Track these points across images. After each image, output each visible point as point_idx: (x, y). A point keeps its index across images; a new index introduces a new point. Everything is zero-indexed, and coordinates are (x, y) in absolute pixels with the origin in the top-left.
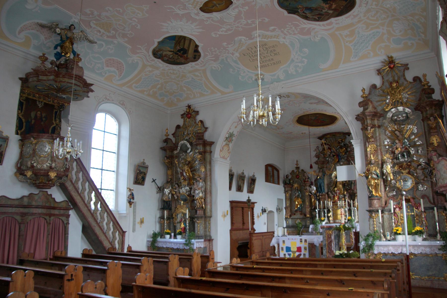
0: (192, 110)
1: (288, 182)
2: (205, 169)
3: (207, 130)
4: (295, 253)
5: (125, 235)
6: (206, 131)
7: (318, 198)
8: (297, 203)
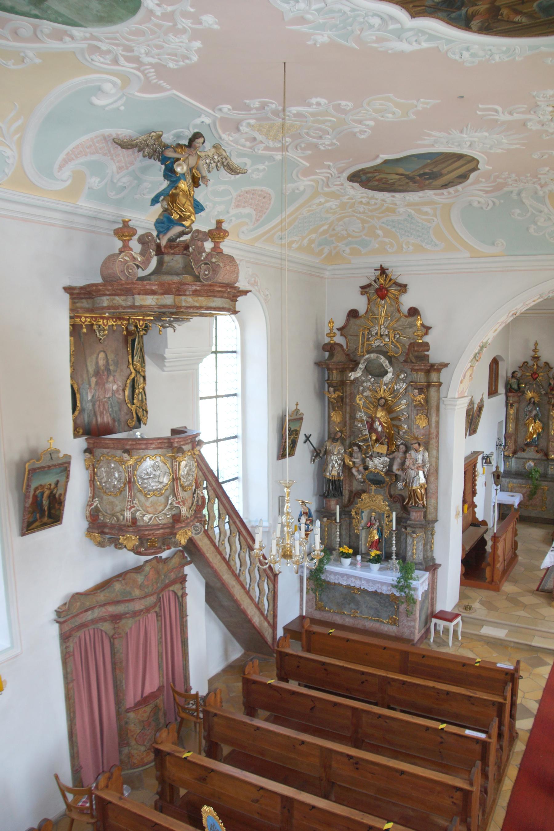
0: (390, 280)
1: (515, 386)
2: (428, 422)
3: (430, 331)
6: (426, 334)
8: (531, 429)
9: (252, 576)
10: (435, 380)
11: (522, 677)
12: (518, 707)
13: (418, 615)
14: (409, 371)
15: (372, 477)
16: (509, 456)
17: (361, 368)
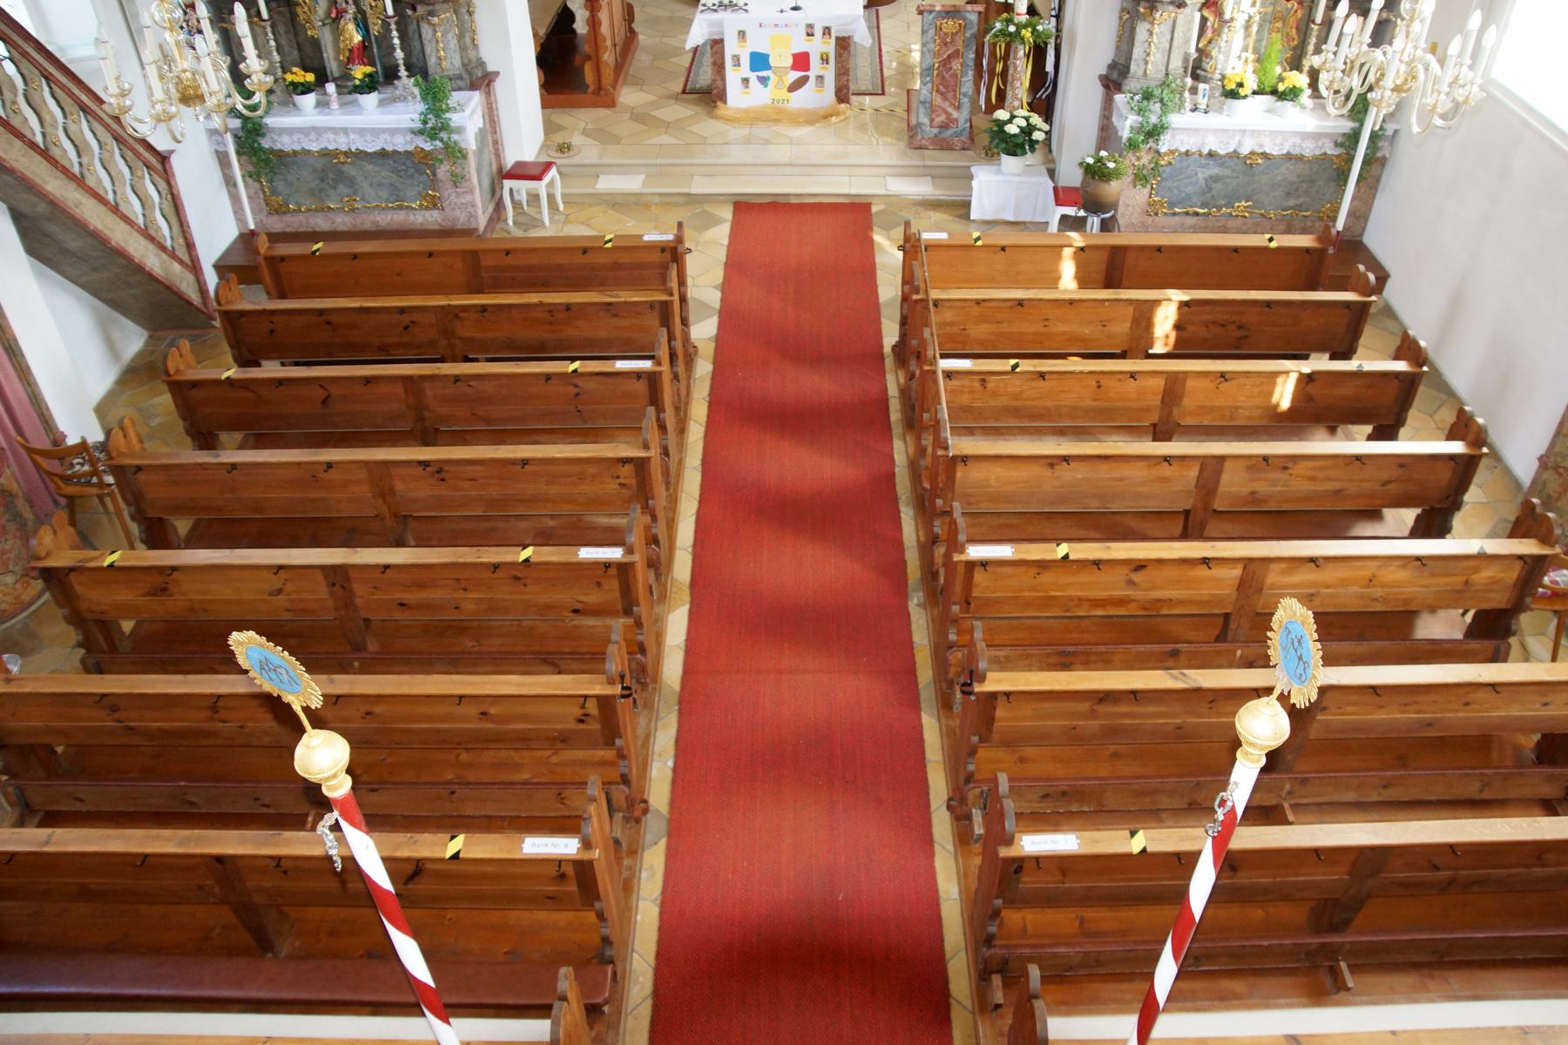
4: (787, 73)
5: (171, 167)
9: (113, 174)
12: (691, 303)
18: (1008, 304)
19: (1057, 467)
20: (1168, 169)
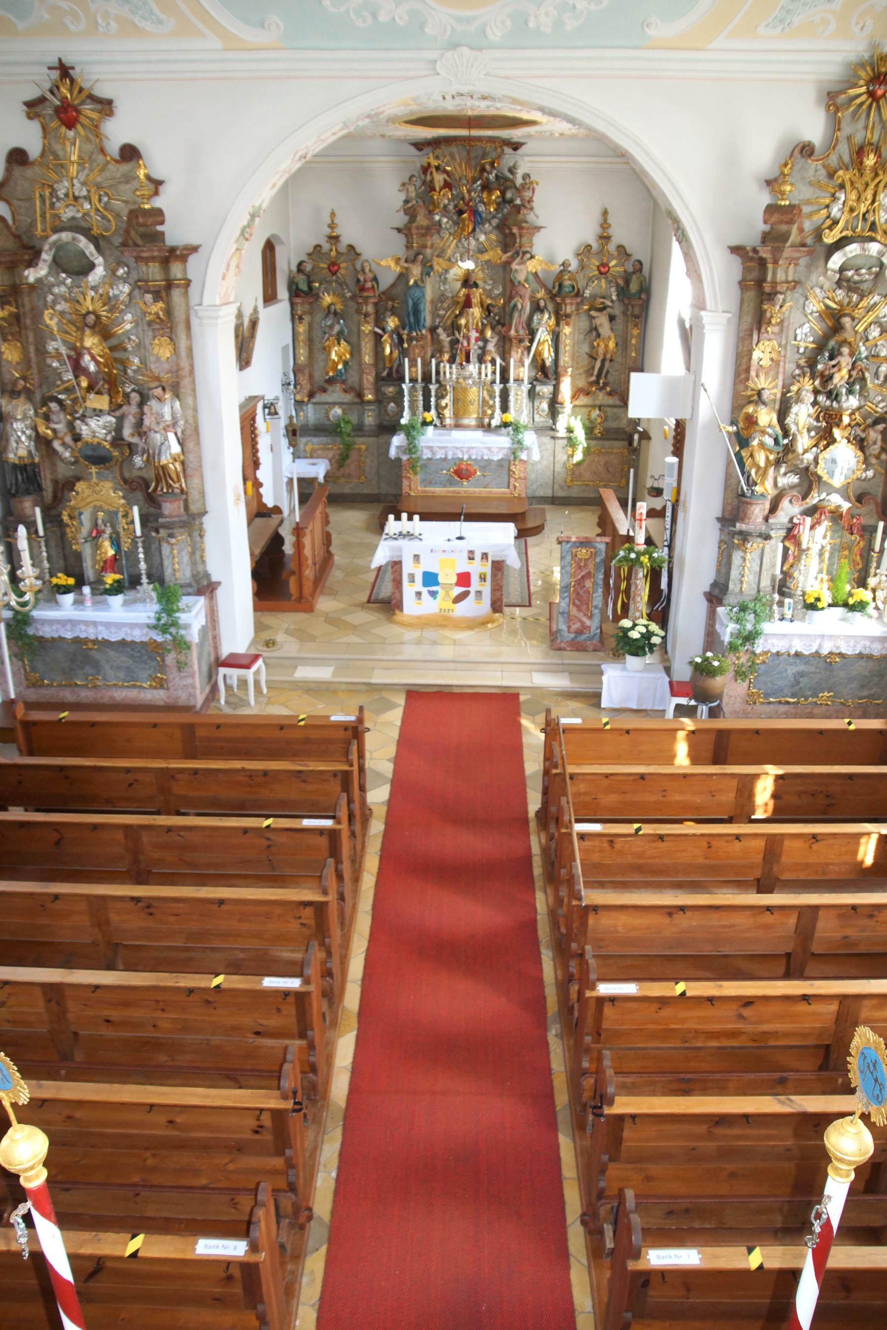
1: (304, 287)
2: (174, 349)
3: (162, 188)
6: (156, 193)
7: (406, 345)
8: (334, 356)
10: (179, 276)
11: (369, 730)
12: (368, 774)
13: (196, 667)
14: (132, 262)
15: (89, 453)
16: (303, 402)
17: (45, 261)
18: (632, 778)
19: (674, 916)
20: (763, 667)
